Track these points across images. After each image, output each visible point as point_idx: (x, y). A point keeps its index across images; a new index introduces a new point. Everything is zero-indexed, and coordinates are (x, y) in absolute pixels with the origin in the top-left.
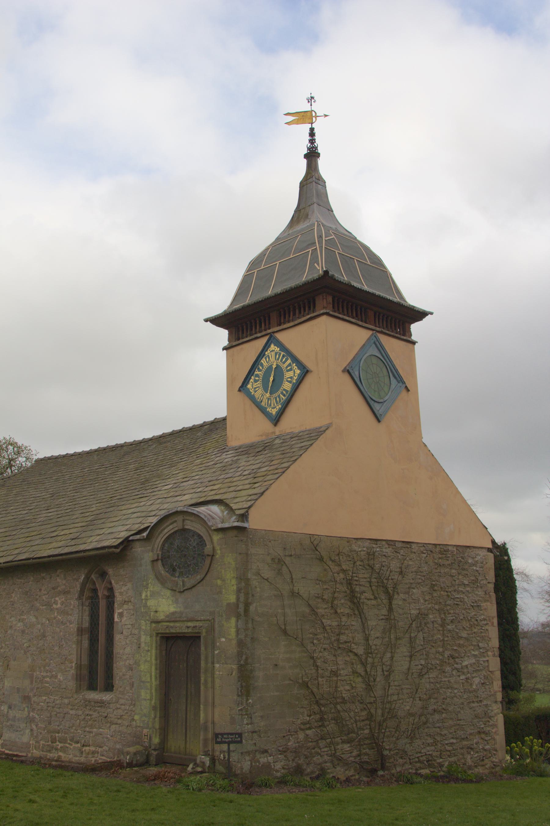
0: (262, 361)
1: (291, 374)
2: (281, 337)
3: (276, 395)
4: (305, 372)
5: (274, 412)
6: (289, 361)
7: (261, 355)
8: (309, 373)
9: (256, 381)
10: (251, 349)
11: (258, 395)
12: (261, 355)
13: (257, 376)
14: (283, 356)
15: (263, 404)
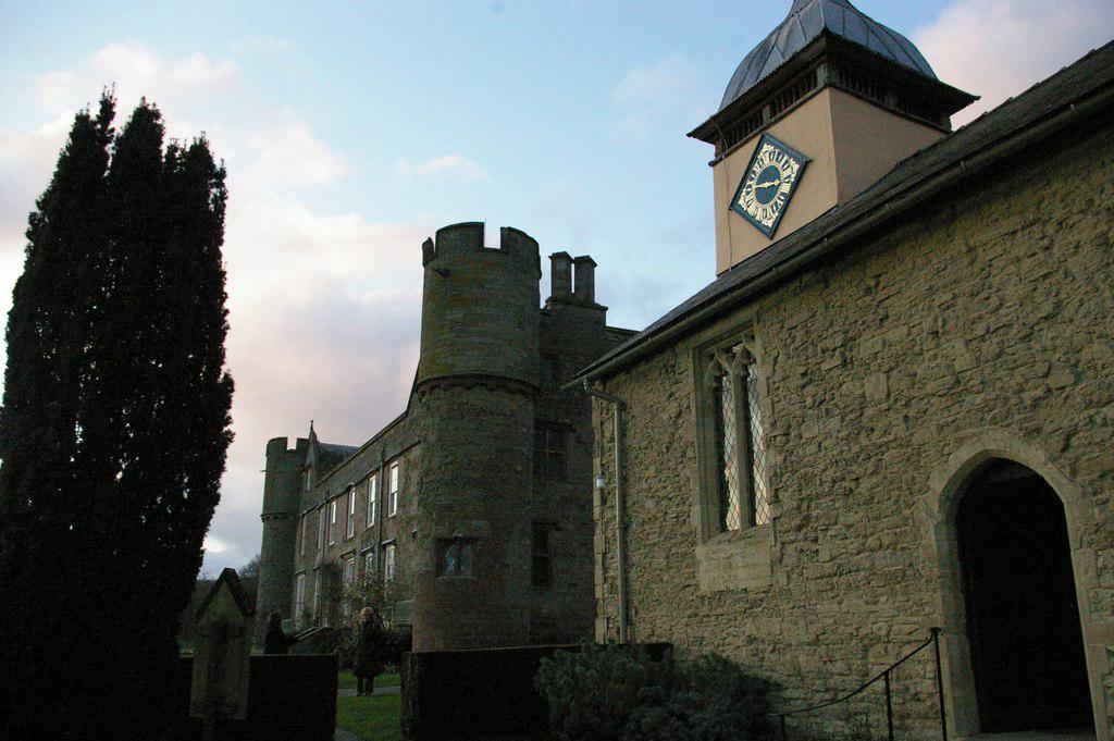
0: (754, 169)
1: (788, 172)
2: (777, 130)
3: (772, 202)
4: (805, 165)
5: (770, 223)
6: (786, 158)
7: (753, 159)
8: (810, 165)
9: (748, 193)
10: (742, 155)
11: (751, 211)
12: (753, 159)
13: (750, 186)
14: (779, 154)
15: (757, 218)
